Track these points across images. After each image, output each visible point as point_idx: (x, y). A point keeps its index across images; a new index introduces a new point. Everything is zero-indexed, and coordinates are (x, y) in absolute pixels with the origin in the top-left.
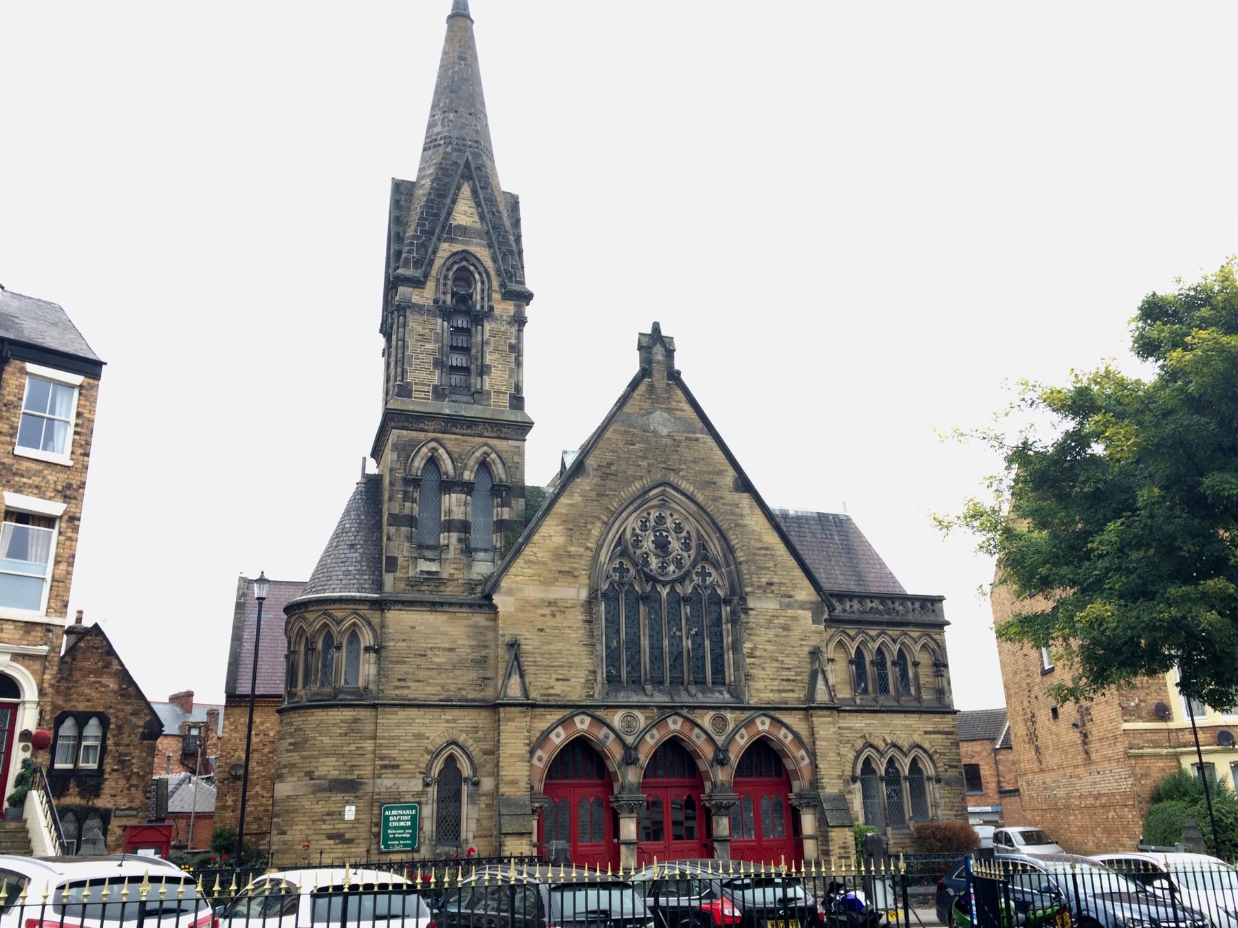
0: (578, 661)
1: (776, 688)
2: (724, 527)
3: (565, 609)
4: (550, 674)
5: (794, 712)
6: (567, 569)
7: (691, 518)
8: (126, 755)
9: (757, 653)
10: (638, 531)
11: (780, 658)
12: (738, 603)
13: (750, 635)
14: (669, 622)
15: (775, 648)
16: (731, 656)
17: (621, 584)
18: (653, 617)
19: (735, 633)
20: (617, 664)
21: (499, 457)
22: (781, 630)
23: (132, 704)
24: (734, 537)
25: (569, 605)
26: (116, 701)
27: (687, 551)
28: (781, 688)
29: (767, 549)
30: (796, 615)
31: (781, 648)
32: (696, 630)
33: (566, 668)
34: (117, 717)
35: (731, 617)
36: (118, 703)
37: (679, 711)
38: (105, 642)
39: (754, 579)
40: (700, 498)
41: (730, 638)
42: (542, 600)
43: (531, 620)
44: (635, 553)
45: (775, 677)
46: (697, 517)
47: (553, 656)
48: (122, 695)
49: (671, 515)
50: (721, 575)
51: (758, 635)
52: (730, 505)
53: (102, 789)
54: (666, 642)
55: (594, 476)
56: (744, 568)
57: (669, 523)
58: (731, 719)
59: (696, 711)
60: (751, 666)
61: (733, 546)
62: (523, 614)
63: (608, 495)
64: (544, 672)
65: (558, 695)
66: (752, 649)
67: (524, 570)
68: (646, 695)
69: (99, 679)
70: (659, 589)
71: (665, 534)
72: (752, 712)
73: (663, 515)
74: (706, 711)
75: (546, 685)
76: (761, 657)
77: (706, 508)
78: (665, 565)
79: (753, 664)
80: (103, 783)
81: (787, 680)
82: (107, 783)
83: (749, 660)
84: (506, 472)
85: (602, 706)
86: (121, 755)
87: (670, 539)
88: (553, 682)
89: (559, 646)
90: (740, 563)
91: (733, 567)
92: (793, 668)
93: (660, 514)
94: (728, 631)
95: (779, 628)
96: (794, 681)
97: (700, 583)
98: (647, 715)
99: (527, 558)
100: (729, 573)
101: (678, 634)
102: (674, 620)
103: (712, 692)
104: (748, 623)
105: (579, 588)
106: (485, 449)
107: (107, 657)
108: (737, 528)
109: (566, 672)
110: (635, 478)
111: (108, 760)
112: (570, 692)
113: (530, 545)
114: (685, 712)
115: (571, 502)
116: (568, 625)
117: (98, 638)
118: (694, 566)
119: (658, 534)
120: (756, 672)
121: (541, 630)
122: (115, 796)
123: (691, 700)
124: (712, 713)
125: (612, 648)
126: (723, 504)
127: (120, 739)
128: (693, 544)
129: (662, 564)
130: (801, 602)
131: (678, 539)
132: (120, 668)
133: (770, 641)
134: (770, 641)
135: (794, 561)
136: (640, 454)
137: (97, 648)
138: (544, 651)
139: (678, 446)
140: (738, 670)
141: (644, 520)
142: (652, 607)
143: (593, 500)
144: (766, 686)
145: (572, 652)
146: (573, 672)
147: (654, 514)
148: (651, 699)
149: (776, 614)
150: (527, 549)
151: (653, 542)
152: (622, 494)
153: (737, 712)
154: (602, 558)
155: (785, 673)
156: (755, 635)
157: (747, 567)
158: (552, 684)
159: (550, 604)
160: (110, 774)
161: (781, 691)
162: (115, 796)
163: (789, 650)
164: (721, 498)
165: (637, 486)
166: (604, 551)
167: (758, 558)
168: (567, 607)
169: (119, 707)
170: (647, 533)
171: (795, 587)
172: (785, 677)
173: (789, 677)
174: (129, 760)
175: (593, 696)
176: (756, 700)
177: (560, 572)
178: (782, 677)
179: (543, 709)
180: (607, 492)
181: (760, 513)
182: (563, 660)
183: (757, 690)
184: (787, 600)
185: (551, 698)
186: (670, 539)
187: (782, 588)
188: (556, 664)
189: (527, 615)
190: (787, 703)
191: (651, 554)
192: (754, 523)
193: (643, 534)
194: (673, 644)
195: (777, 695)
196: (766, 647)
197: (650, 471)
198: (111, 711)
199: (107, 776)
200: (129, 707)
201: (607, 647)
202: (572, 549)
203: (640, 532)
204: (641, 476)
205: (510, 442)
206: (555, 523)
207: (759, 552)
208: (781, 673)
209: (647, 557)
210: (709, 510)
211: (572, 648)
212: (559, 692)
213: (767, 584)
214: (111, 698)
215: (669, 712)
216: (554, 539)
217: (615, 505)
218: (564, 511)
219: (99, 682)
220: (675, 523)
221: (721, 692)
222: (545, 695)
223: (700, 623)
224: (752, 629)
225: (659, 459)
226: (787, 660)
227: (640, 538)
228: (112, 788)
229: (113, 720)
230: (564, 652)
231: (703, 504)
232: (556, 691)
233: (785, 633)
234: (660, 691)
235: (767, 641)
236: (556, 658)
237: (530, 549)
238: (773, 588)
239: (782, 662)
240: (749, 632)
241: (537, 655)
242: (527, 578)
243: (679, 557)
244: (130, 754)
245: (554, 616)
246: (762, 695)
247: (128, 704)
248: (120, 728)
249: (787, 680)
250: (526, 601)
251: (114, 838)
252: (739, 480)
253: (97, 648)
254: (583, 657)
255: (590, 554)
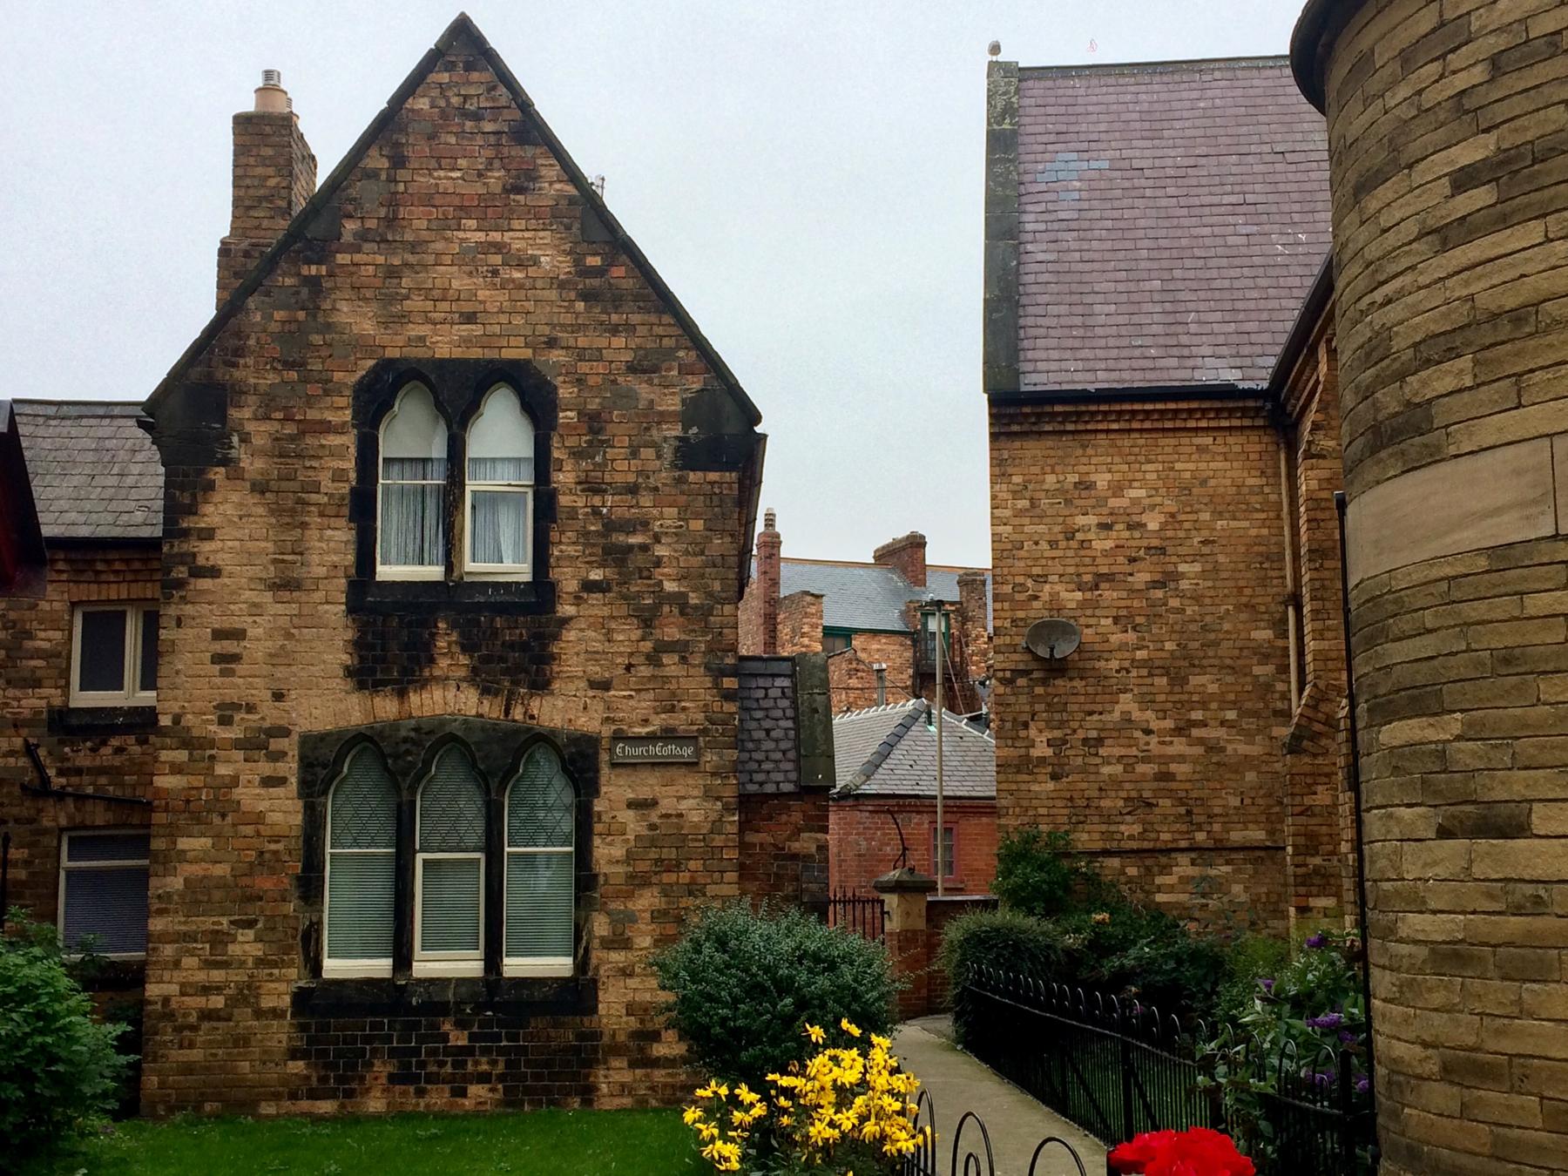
8: (629, 527)
23: (630, 328)
26: (568, 319)
34: (580, 381)
36: (576, 328)
38: (502, 90)
48: (586, 296)
53: (553, 657)
69: (496, 236)
80: (556, 637)
82: (570, 635)
86: (611, 526)
107: (516, 151)
111: (565, 547)
117: (475, 76)
122: (605, 686)
127: (601, 467)
132: (571, 190)
137: (477, 117)
160: (578, 600)
162: (605, 686)
169: (582, 342)
174: (644, 548)
198: (557, 356)
199: (567, 610)
200: (619, 342)
214: (550, 309)
219: (498, 247)
228: (593, 656)
229: (565, 392)
244: (645, 524)
247: (615, 330)
248: (594, 422)
251: (618, 852)
253: (477, 117)
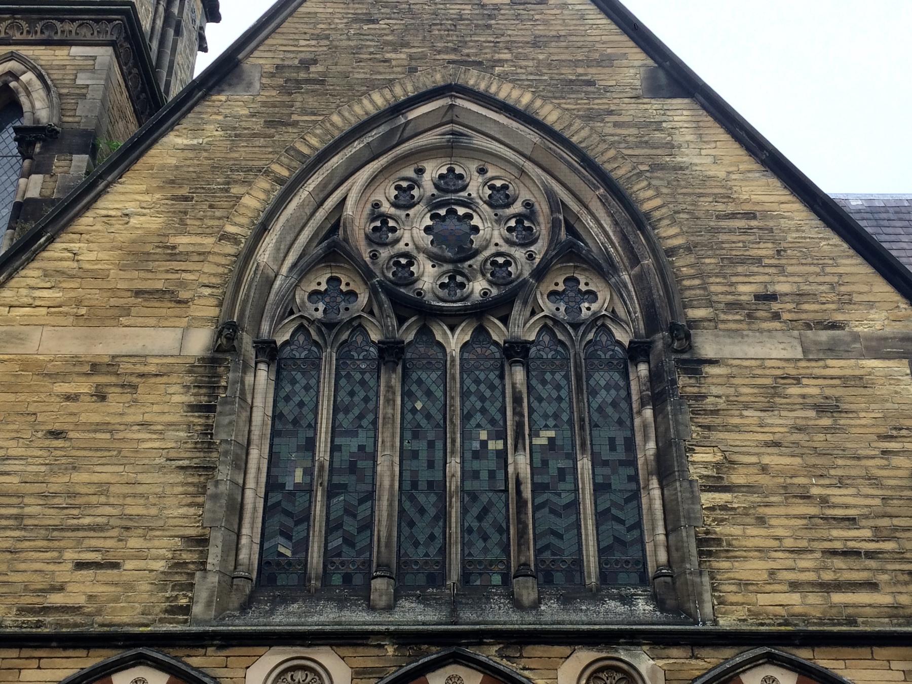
0: (153, 511)
1: (811, 576)
2: (620, 172)
3: (135, 380)
4: (61, 550)
5: (882, 652)
6: (159, 285)
7: (529, 166)
9: (737, 478)
10: (386, 208)
11: (815, 491)
12: (668, 347)
13: (709, 428)
14: (466, 417)
15: (798, 460)
16: (656, 493)
17: (328, 325)
18: (419, 405)
19: (662, 429)
20: (298, 533)
21: (40, 77)
22: (812, 414)
24: (650, 193)
25: (152, 369)
27: (523, 245)
28: (828, 576)
29: (751, 216)
30: (857, 372)
31: (818, 461)
32: (552, 434)
33: (115, 533)
35: (652, 388)
37: (470, 650)
39: (713, 288)
40: (550, 115)
41: (652, 445)
42: (76, 360)
43: (31, 409)
44: (374, 256)
45: (804, 544)
46: (540, 156)
47: (79, 501)
49: (482, 171)
50: (618, 289)
51: (737, 429)
52: (637, 126)
54: (454, 465)
55: (264, 87)
56: (683, 264)
57: (475, 187)
58: (653, 671)
59: (530, 650)
60: (718, 514)
61: (647, 215)
62: (11, 397)
63: (295, 124)
64: (44, 543)
65: (75, 610)
66: (717, 466)
67: (37, 293)
68: (371, 608)
70: (439, 338)
71: (461, 211)
72: (728, 652)
73: (458, 170)
74: (565, 650)
75: (39, 582)
76: (750, 489)
77: (566, 134)
78: (459, 279)
79: (724, 508)
81: (846, 553)
83: (707, 499)
84: (51, 106)
85: (214, 635)
87: (476, 221)
88: (64, 572)
89: (106, 473)
90: (671, 252)
91: (648, 262)
92: (866, 517)
93: (451, 170)
94: (645, 426)
95: (804, 406)
96: (870, 555)
97: (562, 315)
98: (360, 663)
99: (51, 265)
100: (640, 280)
101: (495, 445)
102: (483, 411)
103: (596, 596)
104: (701, 397)
105: (186, 329)
106: (12, 65)
108: (659, 174)
109: (109, 543)
110: (371, 86)
112: (116, 600)
113: (65, 237)
114: (490, 653)
115: (195, 142)
116: (139, 418)
118: (540, 273)
119: (443, 212)
120: (737, 531)
121: (56, 434)
123: (515, 617)
124: (584, 656)
125: (289, 487)
126: (616, 125)
128: (543, 229)
129: (452, 278)
130: (869, 338)
131: (499, 220)
133: (776, 444)
134: (776, 444)
135: (836, 240)
136: (390, 38)
138: (53, 488)
139: (490, 17)
140: (676, 529)
141: (405, 184)
142: (420, 382)
143: (255, 135)
144: (772, 573)
145: (140, 489)
146: (134, 542)
147: (433, 170)
148: (385, 617)
149: (793, 372)
150: (58, 245)
151: (428, 230)
152: (336, 118)
153: (675, 652)
154: (265, 254)
155: (835, 533)
156: (726, 428)
157: (691, 259)
158: (60, 579)
159: (95, 368)
161: (827, 587)
163: (843, 467)
164: (611, 113)
165: (379, 100)
166: (269, 242)
167: (723, 237)
168: (142, 375)
170: (411, 212)
171: (846, 301)
172: (838, 545)
173: (851, 544)
175: (186, 610)
176: (742, 613)
177: (138, 293)
178: (827, 545)
179: (14, 653)
180: (295, 117)
181: (726, 137)
182: (108, 510)
183: (743, 585)
184: (824, 336)
185: (49, 619)
186: (476, 221)
187: (806, 307)
188: (86, 521)
189: (22, 397)
190: (851, 621)
191: (421, 257)
192: (709, 160)
193: (402, 213)
194: (476, 475)
195: (814, 599)
196: (766, 460)
197: (412, 70)
201: (273, 485)
202: (183, 241)
203: (392, 211)
204: (391, 80)
205: (75, 50)
206: (143, 187)
207: (724, 224)
208: (824, 533)
209: (410, 264)
210: (574, 140)
211: (141, 478)
212: (81, 600)
213: (758, 297)
215: (435, 652)
216: (134, 221)
217: (314, 141)
218: (173, 161)
220: (492, 187)
221: (626, 600)
222: (31, 610)
223: (565, 417)
224: (715, 412)
225: (440, 45)
226: (838, 495)
227: (391, 223)
230: (113, 489)
231: (557, 127)
232: (74, 596)
233: (826, 421)
234: (423, 599)
235: (767, 444)
236: (89, 505)
237: (64, 245)
238: (775, 306)
239: (824, 501)
240: (701, 420)
241: (27, 500)
242: (44, 311)
243: (501, 260)
245: (102, 398)
246: (763, 599)
249: (846, 553)
250: (26, 364)
252: (661, 75)
254: (168, 501)
255: (230, 249)
